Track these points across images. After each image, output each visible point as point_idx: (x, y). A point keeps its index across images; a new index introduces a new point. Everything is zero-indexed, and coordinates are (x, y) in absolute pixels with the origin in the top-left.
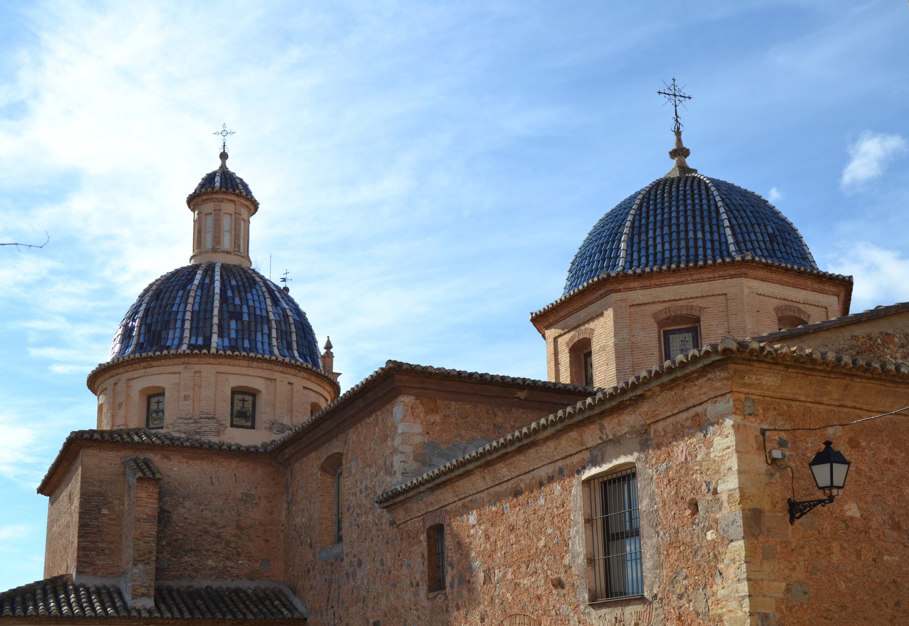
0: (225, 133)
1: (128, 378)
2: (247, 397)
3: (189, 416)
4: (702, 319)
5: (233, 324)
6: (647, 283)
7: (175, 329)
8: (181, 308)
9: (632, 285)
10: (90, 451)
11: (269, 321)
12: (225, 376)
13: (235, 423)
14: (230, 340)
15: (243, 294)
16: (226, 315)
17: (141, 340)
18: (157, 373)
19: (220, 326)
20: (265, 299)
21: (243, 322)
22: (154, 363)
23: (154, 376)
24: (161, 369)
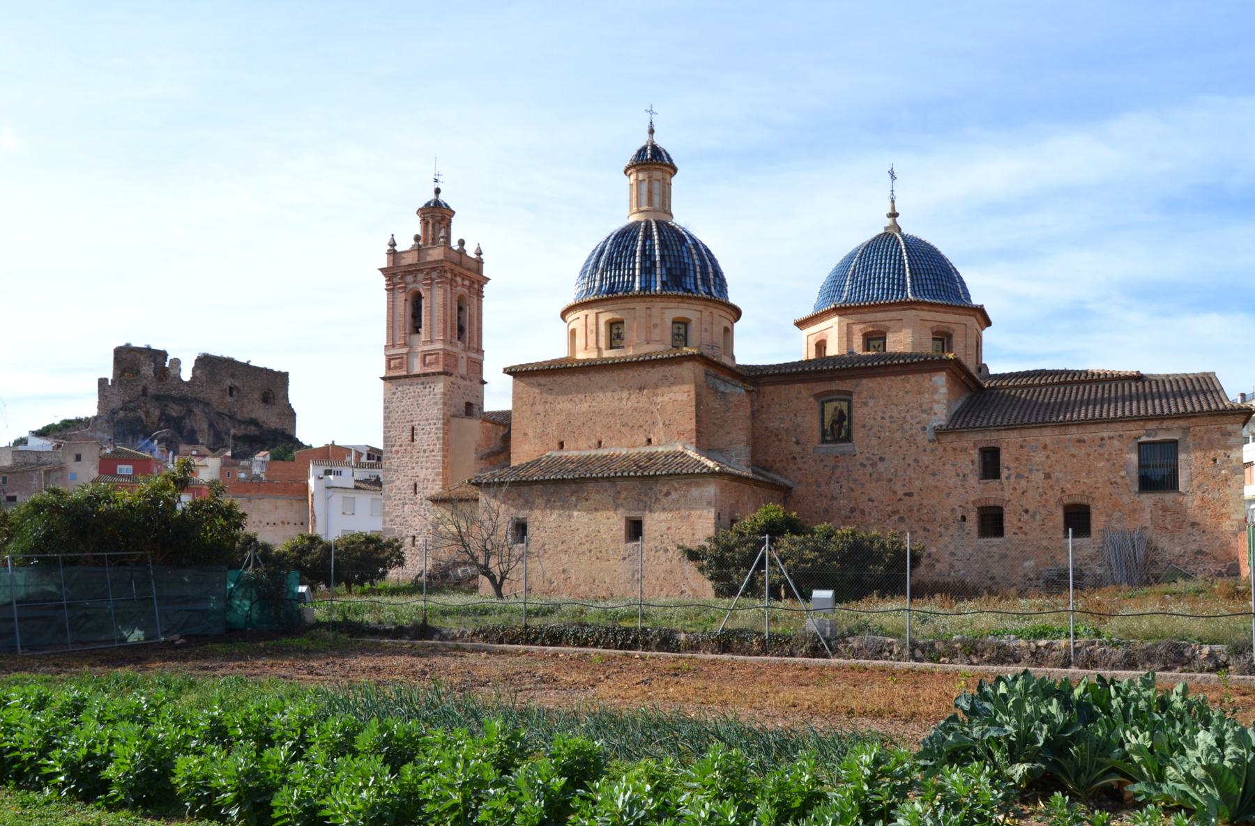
4: (954, 336)
6: (932, 308)
8: (691, 262)
9: (924, 308)
17: (665, 279)
22: (687, 301)
24: (691, 306)
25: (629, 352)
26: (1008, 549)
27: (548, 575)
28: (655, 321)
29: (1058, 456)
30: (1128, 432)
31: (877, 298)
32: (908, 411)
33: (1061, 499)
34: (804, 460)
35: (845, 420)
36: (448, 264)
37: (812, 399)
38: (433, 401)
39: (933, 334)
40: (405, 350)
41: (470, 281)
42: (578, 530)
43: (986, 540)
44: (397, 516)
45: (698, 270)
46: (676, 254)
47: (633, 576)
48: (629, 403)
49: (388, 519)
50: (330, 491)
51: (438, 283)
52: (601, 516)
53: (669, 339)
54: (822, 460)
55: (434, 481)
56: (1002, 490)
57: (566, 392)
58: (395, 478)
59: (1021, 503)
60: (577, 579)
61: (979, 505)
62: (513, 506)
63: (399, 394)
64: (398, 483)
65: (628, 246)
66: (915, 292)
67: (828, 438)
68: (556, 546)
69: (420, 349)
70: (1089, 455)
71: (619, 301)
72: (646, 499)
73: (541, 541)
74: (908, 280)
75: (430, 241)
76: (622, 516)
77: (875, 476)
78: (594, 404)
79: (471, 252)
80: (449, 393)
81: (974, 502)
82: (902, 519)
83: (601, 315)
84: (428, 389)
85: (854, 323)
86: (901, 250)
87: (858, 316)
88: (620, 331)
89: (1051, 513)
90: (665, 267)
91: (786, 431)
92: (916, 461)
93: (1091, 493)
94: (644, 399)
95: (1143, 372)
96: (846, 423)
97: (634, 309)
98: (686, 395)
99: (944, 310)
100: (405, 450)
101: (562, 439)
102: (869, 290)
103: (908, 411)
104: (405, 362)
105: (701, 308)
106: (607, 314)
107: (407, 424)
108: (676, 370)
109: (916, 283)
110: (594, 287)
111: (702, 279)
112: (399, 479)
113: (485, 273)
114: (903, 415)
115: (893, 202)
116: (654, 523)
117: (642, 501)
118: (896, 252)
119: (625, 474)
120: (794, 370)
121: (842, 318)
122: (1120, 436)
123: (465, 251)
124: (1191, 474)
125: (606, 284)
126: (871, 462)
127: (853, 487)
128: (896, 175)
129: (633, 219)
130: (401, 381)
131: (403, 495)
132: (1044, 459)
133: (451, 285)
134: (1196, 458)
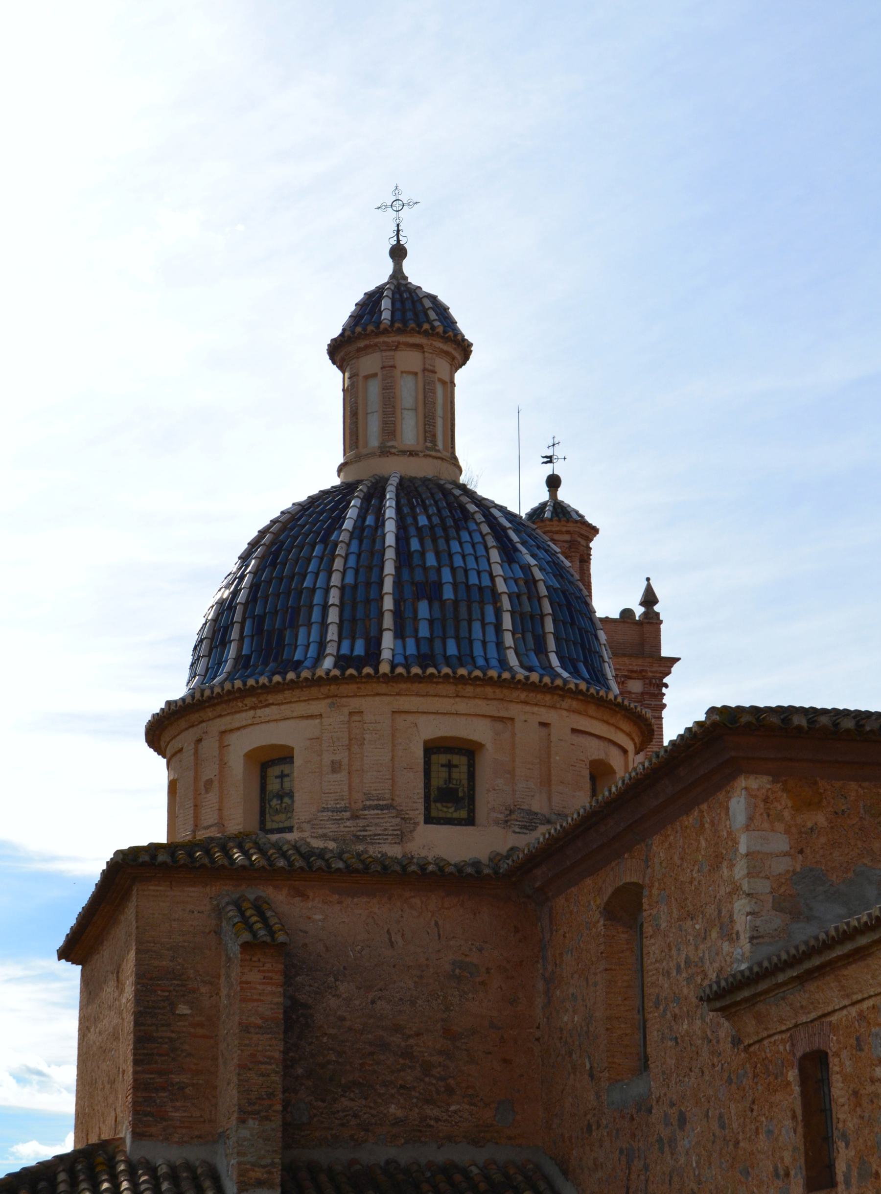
0: (397, 205)
1: (223, 728)
2: (456, 759)
3: (342, 804)
5: (423, 608)
7: (309, 625)
10: (151, 888)
11: (495, 596)
12: (410, 718)
13: (434, 813)
14: (418, 641)
15: (442, 543)
16: (408, 591)
18: (278, 717)
19: (398, 613)
20: (487, 549)
21: (442, 603)
22: (271, 699)
23: (273, 724)
24: (286, 710)
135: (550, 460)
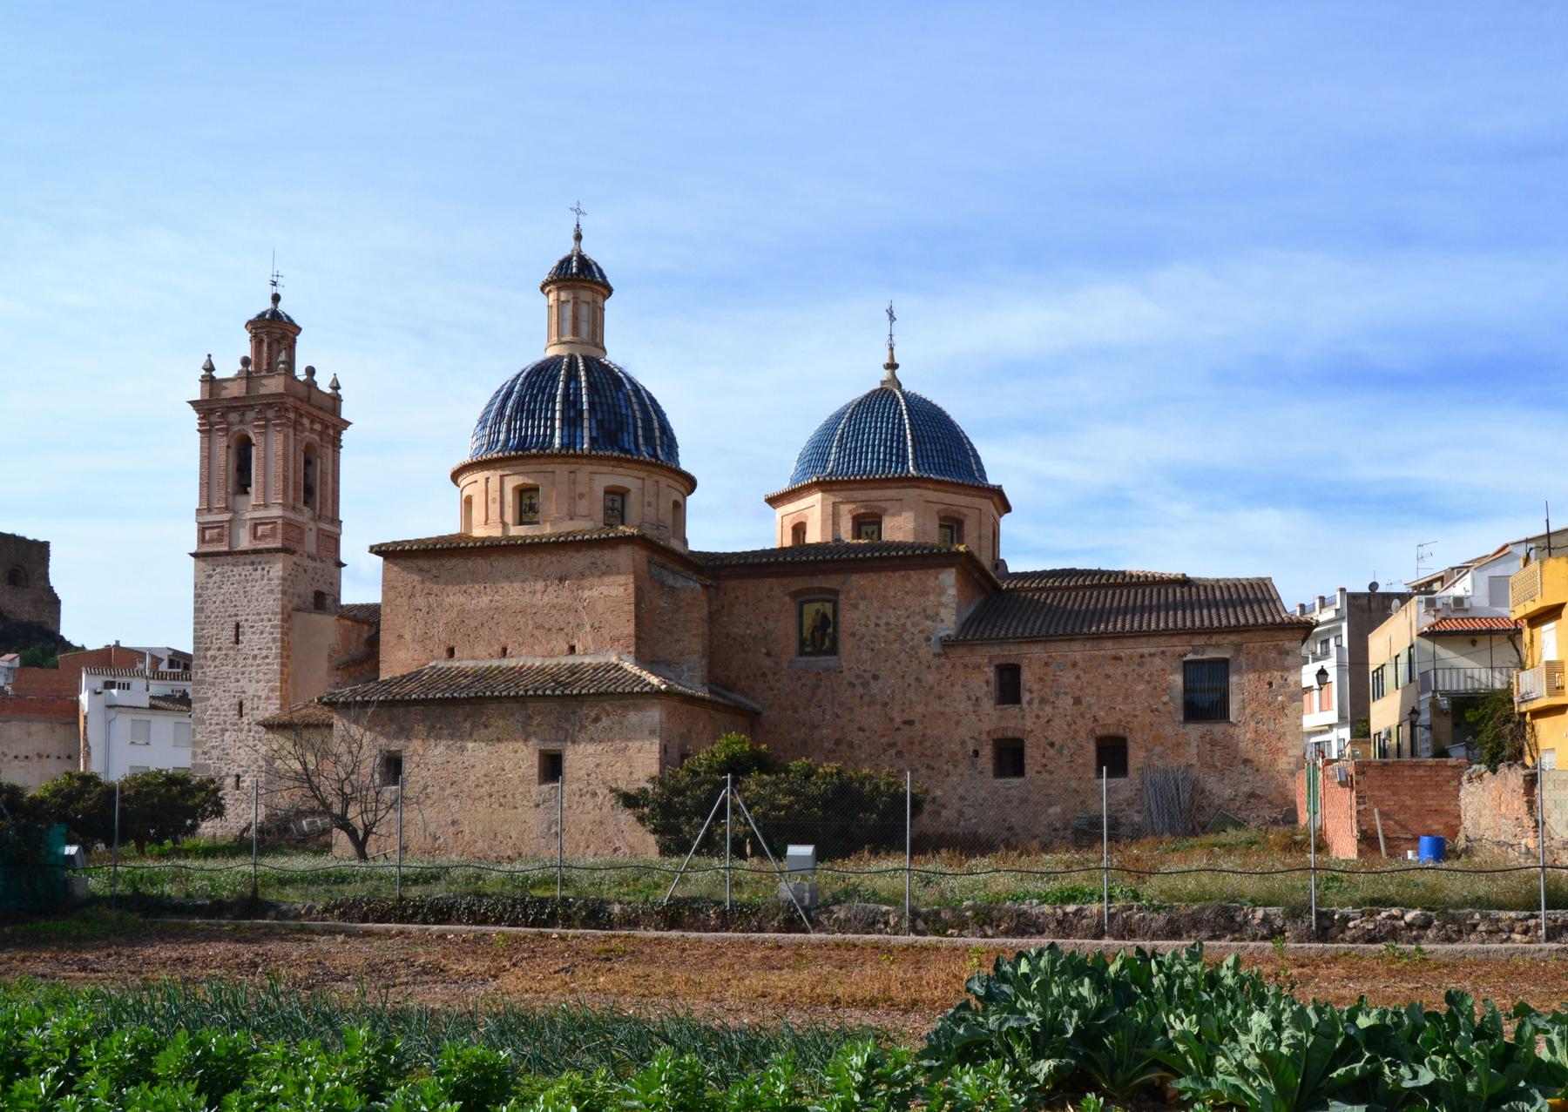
4: (966, 523)
6: (938, 487)
7: (629, 433)
8: (630, 413)
9: (930, 486)
17: (594, 434)
22: (624, 465)
24: (629, 472)
25: (546, 530)
26: (1029, 792)
27: (432, 828)
28: (581, 489)
29: (1091, 675)
30: (1172, 649)
31: (871, 471)
32: (908, 617)
33: (1093, 730)
34: (777, 677)
35: (829, 627)
36: (291, 399)
37: (787, 599)
38: (267, 588)
39: (941, 519)
40: (226, 516)
41: (322, 424)
42: (473, 767)
43: (1003, 780)
44: (213, 747)
45: (640, 424)
46: (610, 401)
47: (549, 828)
48: (546, 599)
49: (199, 751)
50: (113, 712)
51: (276, 425)
52: (506, 748)
53: (600, 515)
54: (799, 678)
55: (268, 698)
56: (1023, 718)
57: (457, 580)
58: (210, 693)
59: (1046, 734)
60: (472, 833)
61: (996, 736)
62: (382, 734)
63: (217, 578)
64: (214, 701)
65: (545, 388)
66: (918, 465)
67: (808, 649)
68: (442, 789)
69: (248, 516)
70: (1126, 676)
71: (532, 461)
72: (567, 726)
73: (422, 783)
74: (910, 450)
75: (265, 367)
76: (535, 749)
77: (867, 699)
78: (496, 597)
79: (324, 385)
80: (290, 578)
81: (988, 733)
82: (900, 754)
83: (506, 479)
84: (259, 571)
85: (842, 503)
86: (901, 411)
87: (848, 494)
88: (533, 501)
89: (1081, 747)
90: (596, 418)
91: (753, 639)
92: (918, 680)
93: (1128, 723)
94: (566, 593)
95: (1192, 574)
96: (830, 630)
97: (553, 472)
98: (622, 589)
99: (955, 490)
100: (226, 655)
101: (452, 644)
102: (860, 461)
103: (908, 617)
104: (226, 533)
105: (643, 475)
106: (516, 477)
107: (228, 620)
108: (608, 555)
109: (919, 454)
110: (498, 441)
111: (644, 436)
112: (216, 696)
113: (344, 416)
114: (902, 621)
115: (892, 349)
116: (580, 758)
117: (562, 728)
118: (895, 414)
119: (540, 692)
120: (764, 560)
121: (826, 496)
122: (1163, 652)
123: (316, 383)
124: (1243, 700)
125: (514, 437)
126: (861, 680)
127: (839, 711)
128: (895, 314)
129: (552, 352)
130: (221, 559)
131: (222, 718)
132: (1073, 680)
133: (295, 429)
134: (1249, 681)
135: (274, 284)
